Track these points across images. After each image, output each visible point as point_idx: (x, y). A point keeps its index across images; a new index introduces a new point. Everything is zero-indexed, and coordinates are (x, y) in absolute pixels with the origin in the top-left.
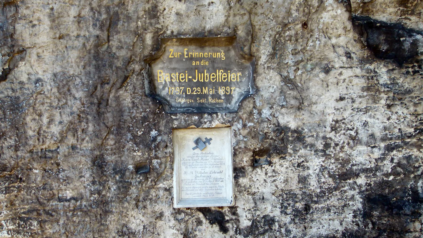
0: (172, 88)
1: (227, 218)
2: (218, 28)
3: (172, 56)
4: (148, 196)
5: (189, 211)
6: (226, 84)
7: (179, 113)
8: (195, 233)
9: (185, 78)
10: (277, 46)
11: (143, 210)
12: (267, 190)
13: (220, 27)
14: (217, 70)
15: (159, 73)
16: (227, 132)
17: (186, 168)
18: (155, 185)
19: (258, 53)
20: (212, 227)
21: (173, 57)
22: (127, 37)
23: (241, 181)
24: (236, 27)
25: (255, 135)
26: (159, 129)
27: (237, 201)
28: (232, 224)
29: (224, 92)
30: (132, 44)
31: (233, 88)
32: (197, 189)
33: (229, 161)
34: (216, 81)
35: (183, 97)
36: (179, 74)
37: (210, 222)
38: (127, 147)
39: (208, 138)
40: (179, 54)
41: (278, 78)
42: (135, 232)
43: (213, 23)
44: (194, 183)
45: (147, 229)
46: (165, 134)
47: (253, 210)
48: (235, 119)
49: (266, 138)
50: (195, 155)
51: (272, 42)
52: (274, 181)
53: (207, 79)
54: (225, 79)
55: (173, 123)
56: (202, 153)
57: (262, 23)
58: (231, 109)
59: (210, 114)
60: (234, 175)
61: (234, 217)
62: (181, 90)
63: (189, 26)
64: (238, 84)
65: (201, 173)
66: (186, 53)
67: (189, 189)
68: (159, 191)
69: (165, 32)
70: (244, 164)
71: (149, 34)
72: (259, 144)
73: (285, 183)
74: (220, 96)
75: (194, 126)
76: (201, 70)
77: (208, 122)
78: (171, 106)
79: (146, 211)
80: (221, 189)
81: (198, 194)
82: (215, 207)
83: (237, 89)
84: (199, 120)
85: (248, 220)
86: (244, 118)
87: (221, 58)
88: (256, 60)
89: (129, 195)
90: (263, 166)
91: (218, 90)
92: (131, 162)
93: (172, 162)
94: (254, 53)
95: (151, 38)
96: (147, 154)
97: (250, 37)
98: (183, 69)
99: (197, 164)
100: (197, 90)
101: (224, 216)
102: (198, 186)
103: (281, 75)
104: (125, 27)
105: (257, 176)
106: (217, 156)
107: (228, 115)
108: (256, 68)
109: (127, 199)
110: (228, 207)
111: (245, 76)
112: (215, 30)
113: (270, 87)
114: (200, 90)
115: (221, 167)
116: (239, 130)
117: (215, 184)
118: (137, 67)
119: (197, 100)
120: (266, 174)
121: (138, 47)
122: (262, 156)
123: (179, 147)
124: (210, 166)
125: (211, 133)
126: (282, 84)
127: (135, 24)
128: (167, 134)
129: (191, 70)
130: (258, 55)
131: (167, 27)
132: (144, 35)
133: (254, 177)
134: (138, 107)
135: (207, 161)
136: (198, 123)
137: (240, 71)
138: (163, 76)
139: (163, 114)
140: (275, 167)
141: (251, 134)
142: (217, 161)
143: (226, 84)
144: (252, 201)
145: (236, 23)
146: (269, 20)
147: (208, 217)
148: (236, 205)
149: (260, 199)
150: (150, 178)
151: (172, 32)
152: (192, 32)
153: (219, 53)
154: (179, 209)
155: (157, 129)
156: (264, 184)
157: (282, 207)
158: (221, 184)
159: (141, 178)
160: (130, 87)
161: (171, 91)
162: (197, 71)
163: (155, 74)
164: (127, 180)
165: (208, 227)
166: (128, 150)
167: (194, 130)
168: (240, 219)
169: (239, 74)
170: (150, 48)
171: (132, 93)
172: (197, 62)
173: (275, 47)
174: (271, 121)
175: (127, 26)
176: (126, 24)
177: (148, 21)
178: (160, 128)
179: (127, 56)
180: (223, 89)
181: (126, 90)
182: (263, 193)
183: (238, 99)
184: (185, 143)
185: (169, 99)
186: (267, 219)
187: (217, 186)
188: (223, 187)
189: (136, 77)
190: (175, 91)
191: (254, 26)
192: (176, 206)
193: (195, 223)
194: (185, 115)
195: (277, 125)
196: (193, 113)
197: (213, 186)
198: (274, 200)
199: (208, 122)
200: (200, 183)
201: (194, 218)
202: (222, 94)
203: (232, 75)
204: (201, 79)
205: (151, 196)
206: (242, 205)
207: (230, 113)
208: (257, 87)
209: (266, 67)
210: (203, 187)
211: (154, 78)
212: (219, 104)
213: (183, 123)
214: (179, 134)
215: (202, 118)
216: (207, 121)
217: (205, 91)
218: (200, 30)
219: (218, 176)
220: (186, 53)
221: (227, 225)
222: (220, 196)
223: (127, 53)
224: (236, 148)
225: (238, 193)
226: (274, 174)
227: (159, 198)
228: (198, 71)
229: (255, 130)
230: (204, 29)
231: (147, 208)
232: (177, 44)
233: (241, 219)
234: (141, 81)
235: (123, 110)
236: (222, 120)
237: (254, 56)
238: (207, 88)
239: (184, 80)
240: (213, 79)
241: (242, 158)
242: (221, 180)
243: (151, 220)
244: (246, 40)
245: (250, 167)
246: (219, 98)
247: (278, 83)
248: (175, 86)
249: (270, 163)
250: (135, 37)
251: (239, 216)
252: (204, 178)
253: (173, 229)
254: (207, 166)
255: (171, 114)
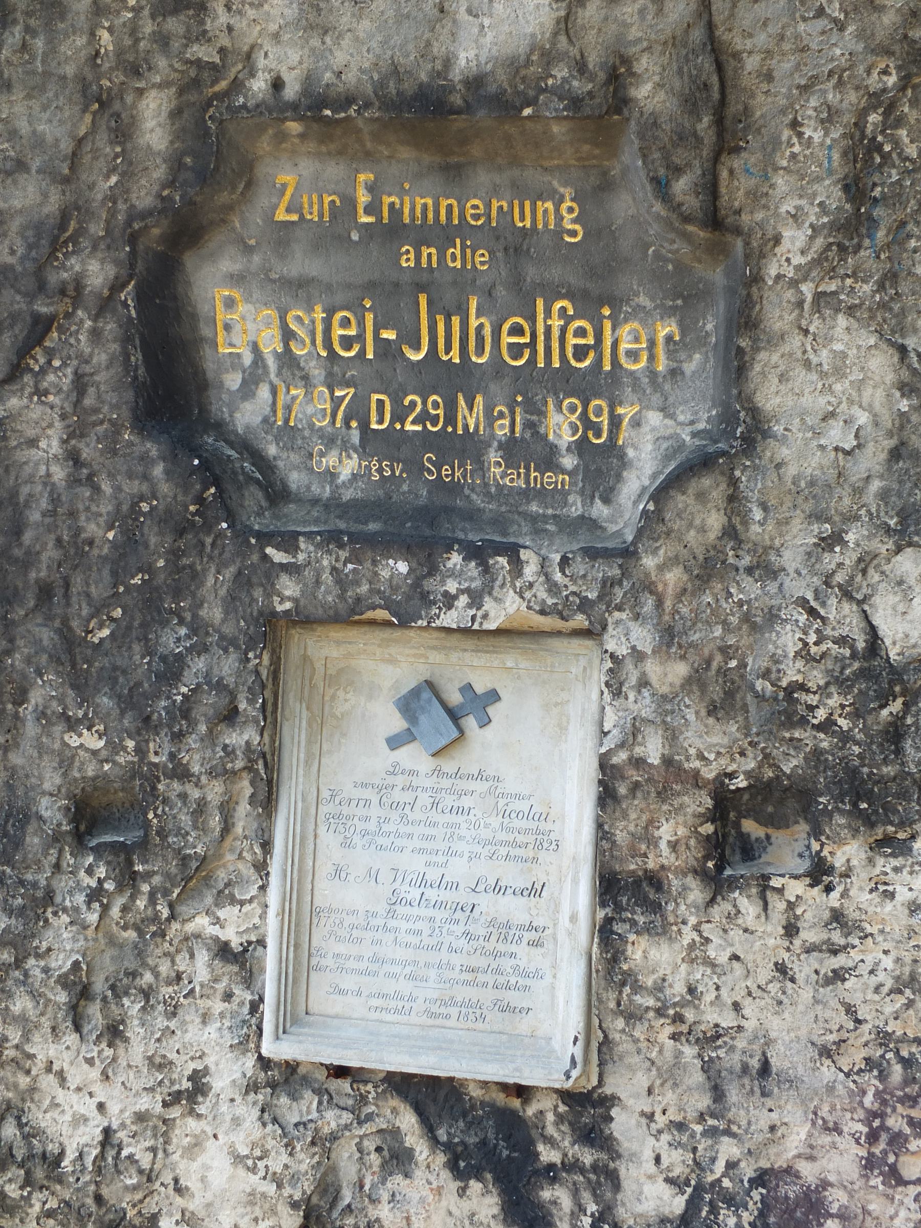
0: (293, 392)
1: (548, 1155)
2: (515, 66)
3: (288, 210)
4: (134, 974)
5: (345, 1085)
6: (590, 384)
7: (309, 535)
8: (373, 1213)
9: (361, 337)
10: (876, 178)
11: (104, 1045)
12: (788, 1028)
13: (528, 63)
14: (540, 303)
15: (219, 306)
16: (583, 662)
17: (347, 844)
18: (173, 917)
19: (759, 216)
20: (462, 1192)
21: (295, 217)
22: (44, 108)
23: (638, 955)
24: (626, 61)
25: (730, 694)
26: (195, 616)
27: (609, 1067)
28: (575, 1194)
29: (575, 430)
30: (66, 146)
31: (626, 411)
32: (397, 969)
33: (578, 832)
34: (532, 361)
35: (346, 447)
36: (330, 312)
37: (452, 1166)
38: (36, 697)
39: (480, 689)
40: (327, 199)
41: (881, 365)
42: (62, 1154)
43: (489, 37)
44: (378, 936)
45: (120, 1148)
46: (227, 643)
47: (698, 1128)
48: (619, 594)
49: (789, 717)
50: (400, 780)
51: (845, 154)
52: (838, 976)
53: (480, 351)
54: (580, 352)
55: (271, 591)
56: (438, 772)
57: (782, 37)
58: (612, 528)
59: (477, 554)
60: (601, 914)
61: (587, 1157)
62: (337, 402)
63: (353, 56)
64: (659, 386)
65: (423, 882)
66: (363, 198)
67: (352, 964)
68: (192, 956)
69: (237, 85)
70: (662, 856)
71: (153, 93)
72: (750, 752)
73: (901, 1001)
74: (553, 449)
75: (382, 614)
76: (449, 297)
77: (463, 600)
78: (277, 494)
79: (121, 1051)
80: (526, 988)
81: (398, 996)
82: (485, 1084)
83: (654, 418)
84: (417, 584)
85: (668, 1180)
86: (670, 591)
87: (560, 232)
88: (747, 256)
89: (38, 956)
90: (776, 882)
91: (542, 414)
92: (52, 780)
93: (267, 800)
94: (738, 212)
95: (164, 114)
96: (130, 744)
97: (706, 120)
98: (349, 286)
99: (403, 829)
100: (422, 412)
101: (532, 1143)
102: (400, 954)
103: (903, 350)
104: (33, 57)
105: (735, 934)
106: (518, 797)
107: (579, 566)
108: (749, 301)
109: (26, 975)
110: (557, 1091)
111: (702, 341)
112: (502, 77)
113: (832, 415)
114: (440, 412)
115: (535, 860)
116: (638, 656)
117: (496, 955)
118: (97, 273)
119: (423, 468)
120: (791, 930)
121: (101, 164)
122: (777, 821)
123: (320, 723)
124: (478, 849)
125: (495, 660)
126: (904, 405)
127: (81, 41)
128: (237, 647)
129: (392, 296)
130: (760, 225)
131: (249, 56)
132: (129, 99)
133: (716, 940)
134: (97, 489)
135: (460, 819)
136: (409, 598)
137: (670, 312)
138: (241, 323)
139: (221, 535)
140: (845, 894)
141: (703, 688)
142: (517, 824)
143: (590, 384)
144: (698, 1077)
145: (620, 38)
146: (822, 23)
147: (444, 1138)
148: (608, 1090)
149: (745, 1069)
150: (148, 875)
151: (277, 84)
152: (381, 85)
153: (549, 205)
154: (291, 1067)
155: (188, 616)
156: (774, 988)
157: (873, 1137)
158: (526, 956)
159: (101, 872)
160: (61, 379)
161: (288, 408)
162: (423, 300)
163: (203, 309)
164: (29, 877)
165: (439, 1191)
166: (42, 714)
167: (387, 633)
168: (623, 1173)
169: (666, 329)
170: (160, 172)
171: (69, 408)
172: (425, 251)
173: (857, 179)
174: (823, 619)
175: (45, 55)
176: (39, 44)
177: (148, 27)
178: (203, 613)
179: (46, 210)
180: (572, 409)
181: (41, 393)
182: (769, 1042)
183: (654, 476)
184: (347, 706)
185: (272, 450)
186: (782, 1191)
187: (507, 964)
188: (537, 975)
189: (88, 324)
190: (310, 410)
191: (736, 56)
192: (267, 1049)
193: (374, 1159)
194: (341, 546)
195: (861, 645)
196: (386, 544)
197: (482, 962)
198: (830, 1089)
199: (463, 600)
200: (415, 940)
201: (369, 1128)
202: (567, 438)
203: (625, 331)
204: (448, 350)
205: (148, 977)
206: (637, 1096)
207: (592, 554)
208: (754, 411)
209: (809, 298)
210: (427, 965)
211: (195, 328)
212: (541, 494)
213: (328, 593)
214: (323, 648)
215: (430, 574)
216: (461, 591)
217: (471, 417)
218: (423, 77)
219: (515, 909)
220: (363, 198)
221: (546, 1195)
222: (524, 1025)
223: (45, 195)
224: (615, 760)
225: (620, 1023)
226: (837, 938)
227: (192, 991)
228: (430, 303)
229: (733, 664)
230: (442, 74)
231: (127, 1040)
232: (311, 146)
233: (629, 1173)
234: (115, 347)
235: (22, 499)
236: (542, 594)
237: (737, 231)
238: (479, 399)
239: (356, 348)
240: (516, 351)
241: (651, 822)
242: (533, 935)
243: (144, 1103)
244: (683, 137)
245: (692, 882)
246: (548, 459)
247: (880, 393)
248: (306, 379)
249: (819, 873)
250: (84, 110)
251: (615, 1155)
252: (440, 915)
253: (253, 1170)
254: (461, 846)
255: (265, 538)
